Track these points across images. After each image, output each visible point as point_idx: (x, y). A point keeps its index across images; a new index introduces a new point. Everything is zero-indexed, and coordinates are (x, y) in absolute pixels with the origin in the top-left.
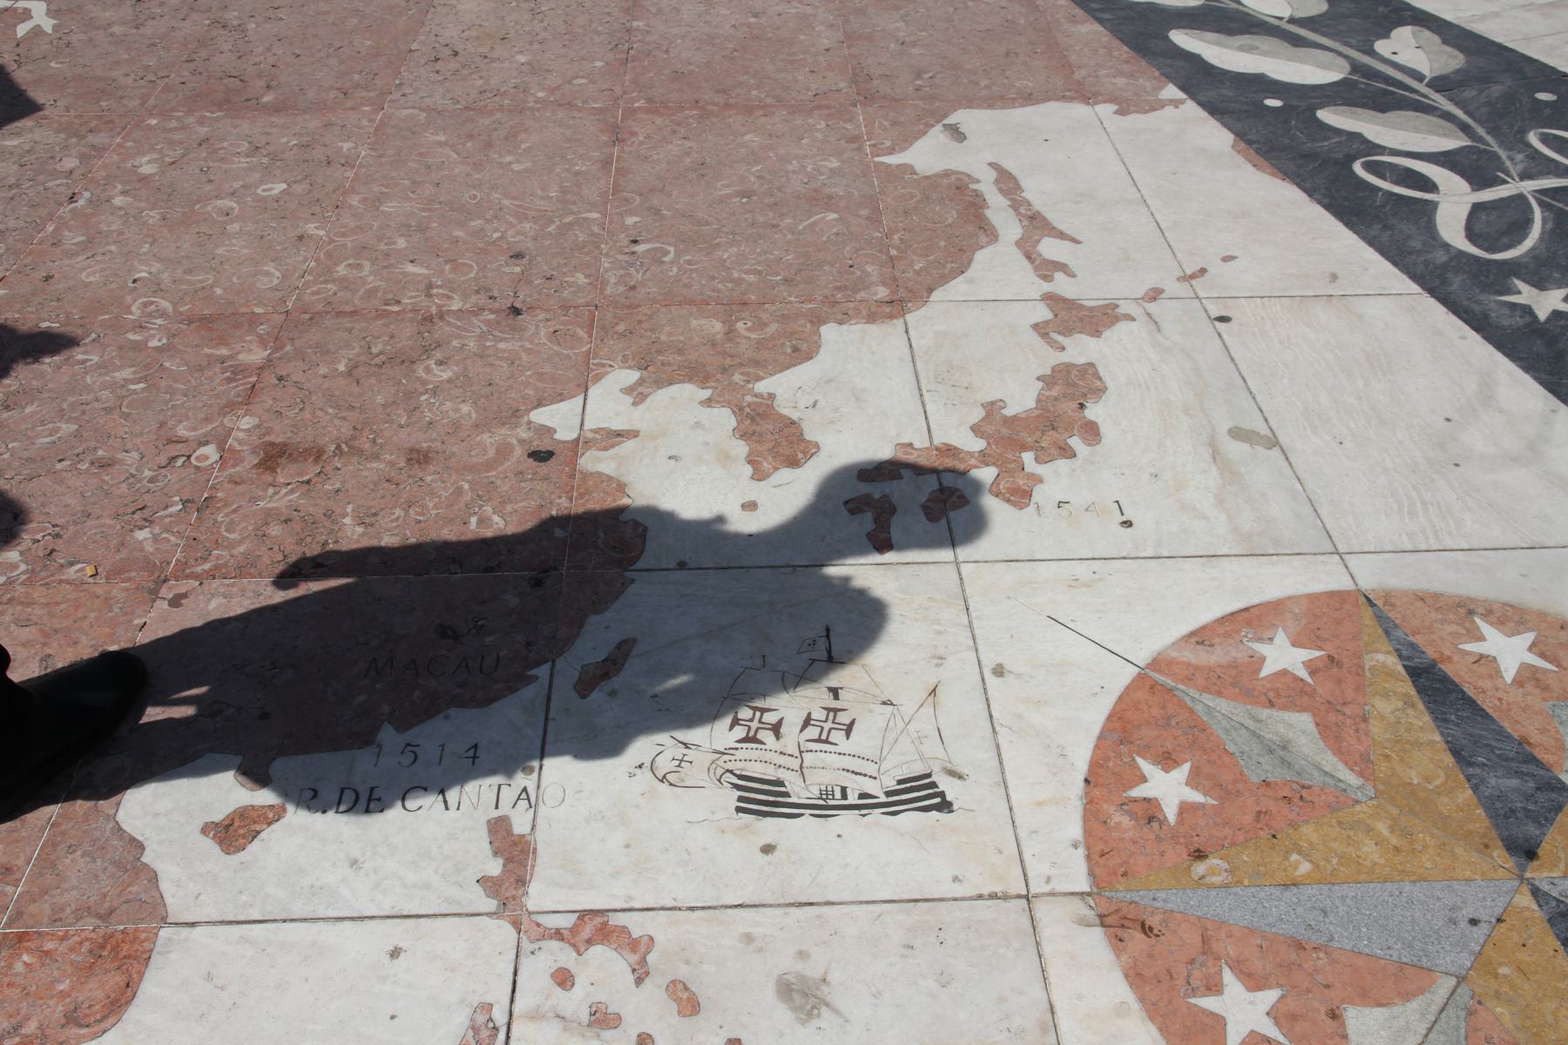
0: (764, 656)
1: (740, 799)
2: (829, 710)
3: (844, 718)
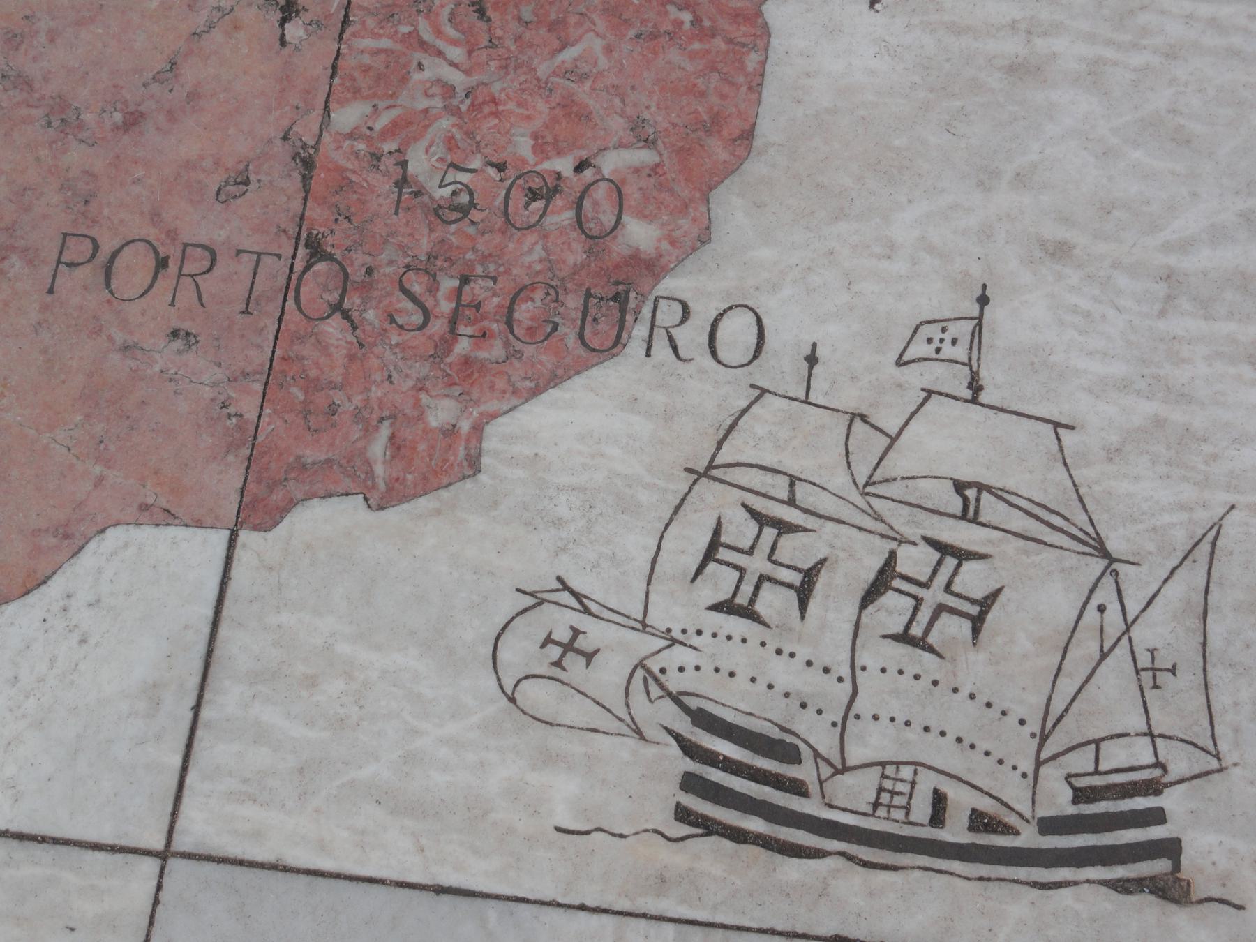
1: (690, 783)
2: (944, 549)
3: (973, 580)
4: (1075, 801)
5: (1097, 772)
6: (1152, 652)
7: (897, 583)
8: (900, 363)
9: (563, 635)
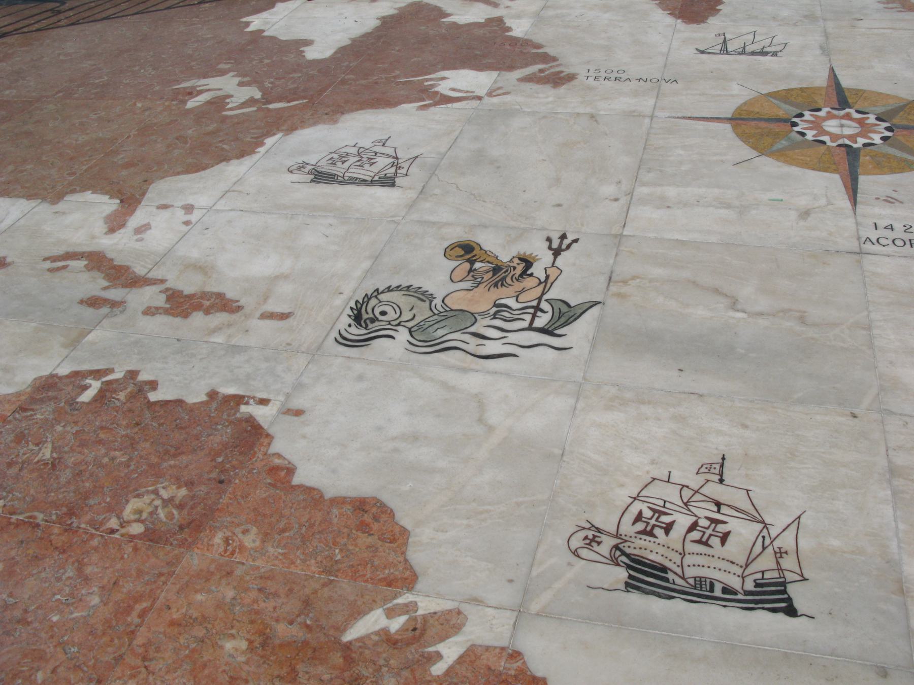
3: (721, 528)
4: (755, 587)
5: (763, 578)
8: (697, 473)
9: (591, 537)
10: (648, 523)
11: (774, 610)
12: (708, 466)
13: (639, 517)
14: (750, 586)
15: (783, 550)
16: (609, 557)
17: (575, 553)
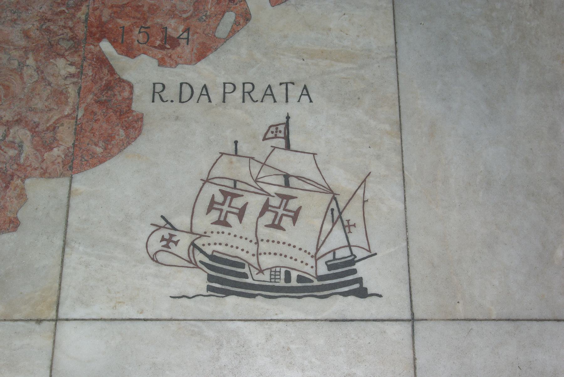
0: (236, 142)
2: (282, 197)
3: (293, 205)
4: (329, 270)
6: (348, 221)
7: (270, 208)
8: (265, 139)
9: (167, 237)
10: (221, 210)
11: (345, 294)
12: (273, 129)
13: (212, 205)
14: (323, 270)
15: (351, 223)
16: (186, 257)
17: (154, 259)
